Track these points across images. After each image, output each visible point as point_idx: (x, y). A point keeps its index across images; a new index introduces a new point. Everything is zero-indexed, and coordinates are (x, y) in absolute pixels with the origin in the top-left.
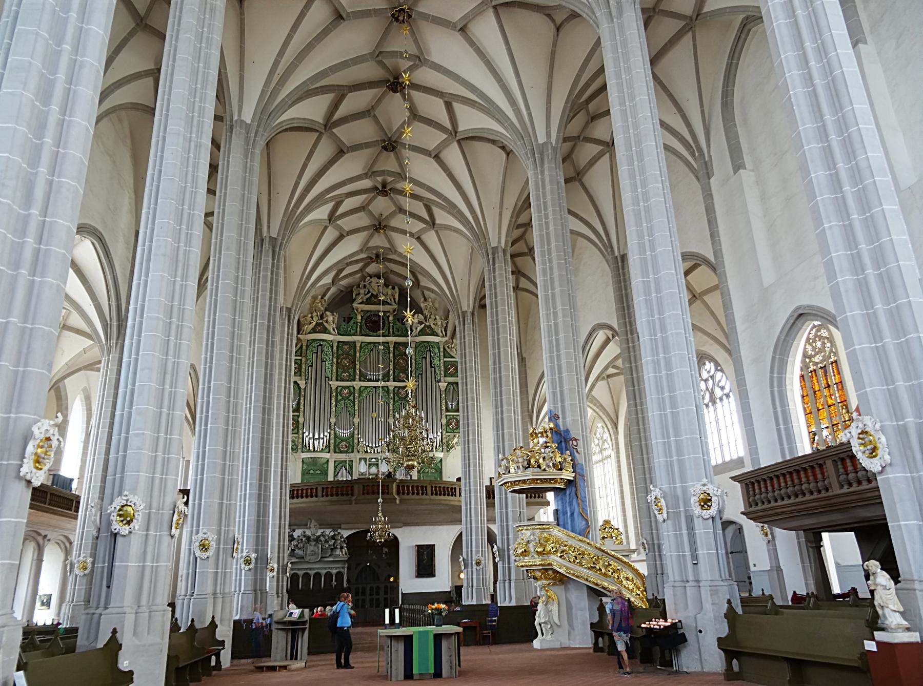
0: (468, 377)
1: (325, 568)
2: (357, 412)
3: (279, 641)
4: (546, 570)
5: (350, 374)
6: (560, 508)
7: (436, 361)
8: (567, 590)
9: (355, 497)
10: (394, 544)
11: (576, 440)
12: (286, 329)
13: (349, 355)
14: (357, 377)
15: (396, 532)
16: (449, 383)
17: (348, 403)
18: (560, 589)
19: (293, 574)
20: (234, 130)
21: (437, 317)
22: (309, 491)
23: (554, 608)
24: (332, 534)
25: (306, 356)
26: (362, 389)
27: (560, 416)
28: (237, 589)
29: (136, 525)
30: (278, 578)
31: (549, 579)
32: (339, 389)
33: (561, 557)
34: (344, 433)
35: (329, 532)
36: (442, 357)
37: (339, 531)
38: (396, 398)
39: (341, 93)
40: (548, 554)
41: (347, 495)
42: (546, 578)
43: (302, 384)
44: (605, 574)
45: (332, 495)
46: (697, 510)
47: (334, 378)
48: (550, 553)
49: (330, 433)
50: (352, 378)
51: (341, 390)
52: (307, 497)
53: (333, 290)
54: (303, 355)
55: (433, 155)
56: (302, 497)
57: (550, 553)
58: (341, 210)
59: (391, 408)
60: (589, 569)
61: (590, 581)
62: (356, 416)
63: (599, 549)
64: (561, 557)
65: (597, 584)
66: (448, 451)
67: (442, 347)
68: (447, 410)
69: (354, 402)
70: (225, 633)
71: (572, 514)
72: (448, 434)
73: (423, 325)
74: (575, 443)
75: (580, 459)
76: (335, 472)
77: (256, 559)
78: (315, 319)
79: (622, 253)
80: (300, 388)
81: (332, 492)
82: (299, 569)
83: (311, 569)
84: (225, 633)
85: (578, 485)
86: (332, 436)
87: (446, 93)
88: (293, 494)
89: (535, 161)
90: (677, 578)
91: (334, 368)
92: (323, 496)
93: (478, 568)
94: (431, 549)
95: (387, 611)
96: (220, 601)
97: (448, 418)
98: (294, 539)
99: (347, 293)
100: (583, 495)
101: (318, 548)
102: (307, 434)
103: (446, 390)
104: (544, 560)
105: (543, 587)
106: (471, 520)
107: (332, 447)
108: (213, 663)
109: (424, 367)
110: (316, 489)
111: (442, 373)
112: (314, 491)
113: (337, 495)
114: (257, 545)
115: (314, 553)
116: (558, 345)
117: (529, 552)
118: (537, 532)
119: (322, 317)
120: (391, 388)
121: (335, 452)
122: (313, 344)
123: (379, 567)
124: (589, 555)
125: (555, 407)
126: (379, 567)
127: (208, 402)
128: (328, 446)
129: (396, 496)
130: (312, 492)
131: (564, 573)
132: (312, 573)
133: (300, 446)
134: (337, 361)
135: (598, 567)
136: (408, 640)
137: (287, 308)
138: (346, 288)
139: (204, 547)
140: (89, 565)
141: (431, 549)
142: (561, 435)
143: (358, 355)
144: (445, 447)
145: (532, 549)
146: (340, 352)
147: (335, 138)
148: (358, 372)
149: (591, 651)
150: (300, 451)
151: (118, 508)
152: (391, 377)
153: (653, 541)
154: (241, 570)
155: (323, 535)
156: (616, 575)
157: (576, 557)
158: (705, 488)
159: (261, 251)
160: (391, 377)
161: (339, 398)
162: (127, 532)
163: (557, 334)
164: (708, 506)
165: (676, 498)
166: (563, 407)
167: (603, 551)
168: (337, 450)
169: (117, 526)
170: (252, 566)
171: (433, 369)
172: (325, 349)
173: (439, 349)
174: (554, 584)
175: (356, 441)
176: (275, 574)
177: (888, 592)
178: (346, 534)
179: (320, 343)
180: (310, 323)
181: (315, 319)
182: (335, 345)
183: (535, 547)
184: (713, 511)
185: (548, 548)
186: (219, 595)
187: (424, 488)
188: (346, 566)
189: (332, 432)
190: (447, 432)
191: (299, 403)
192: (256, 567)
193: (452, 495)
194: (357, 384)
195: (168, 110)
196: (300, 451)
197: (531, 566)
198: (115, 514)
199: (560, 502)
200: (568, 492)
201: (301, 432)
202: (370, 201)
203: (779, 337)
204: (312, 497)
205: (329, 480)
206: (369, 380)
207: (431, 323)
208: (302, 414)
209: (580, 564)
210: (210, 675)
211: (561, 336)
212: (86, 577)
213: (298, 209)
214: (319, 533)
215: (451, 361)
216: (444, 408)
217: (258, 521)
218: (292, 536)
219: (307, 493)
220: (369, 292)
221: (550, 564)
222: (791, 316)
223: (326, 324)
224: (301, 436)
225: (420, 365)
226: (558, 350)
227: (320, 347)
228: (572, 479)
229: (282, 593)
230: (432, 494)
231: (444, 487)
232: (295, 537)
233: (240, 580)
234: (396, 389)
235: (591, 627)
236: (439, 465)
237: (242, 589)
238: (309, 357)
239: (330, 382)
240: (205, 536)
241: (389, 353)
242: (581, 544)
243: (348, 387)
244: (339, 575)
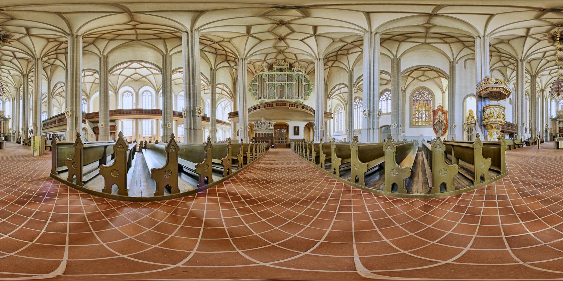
24: (269, 122)
115: (264, 127)
120: (287, 84)
132: (264, 133)
216: (304, 89)
244: (272, 134)
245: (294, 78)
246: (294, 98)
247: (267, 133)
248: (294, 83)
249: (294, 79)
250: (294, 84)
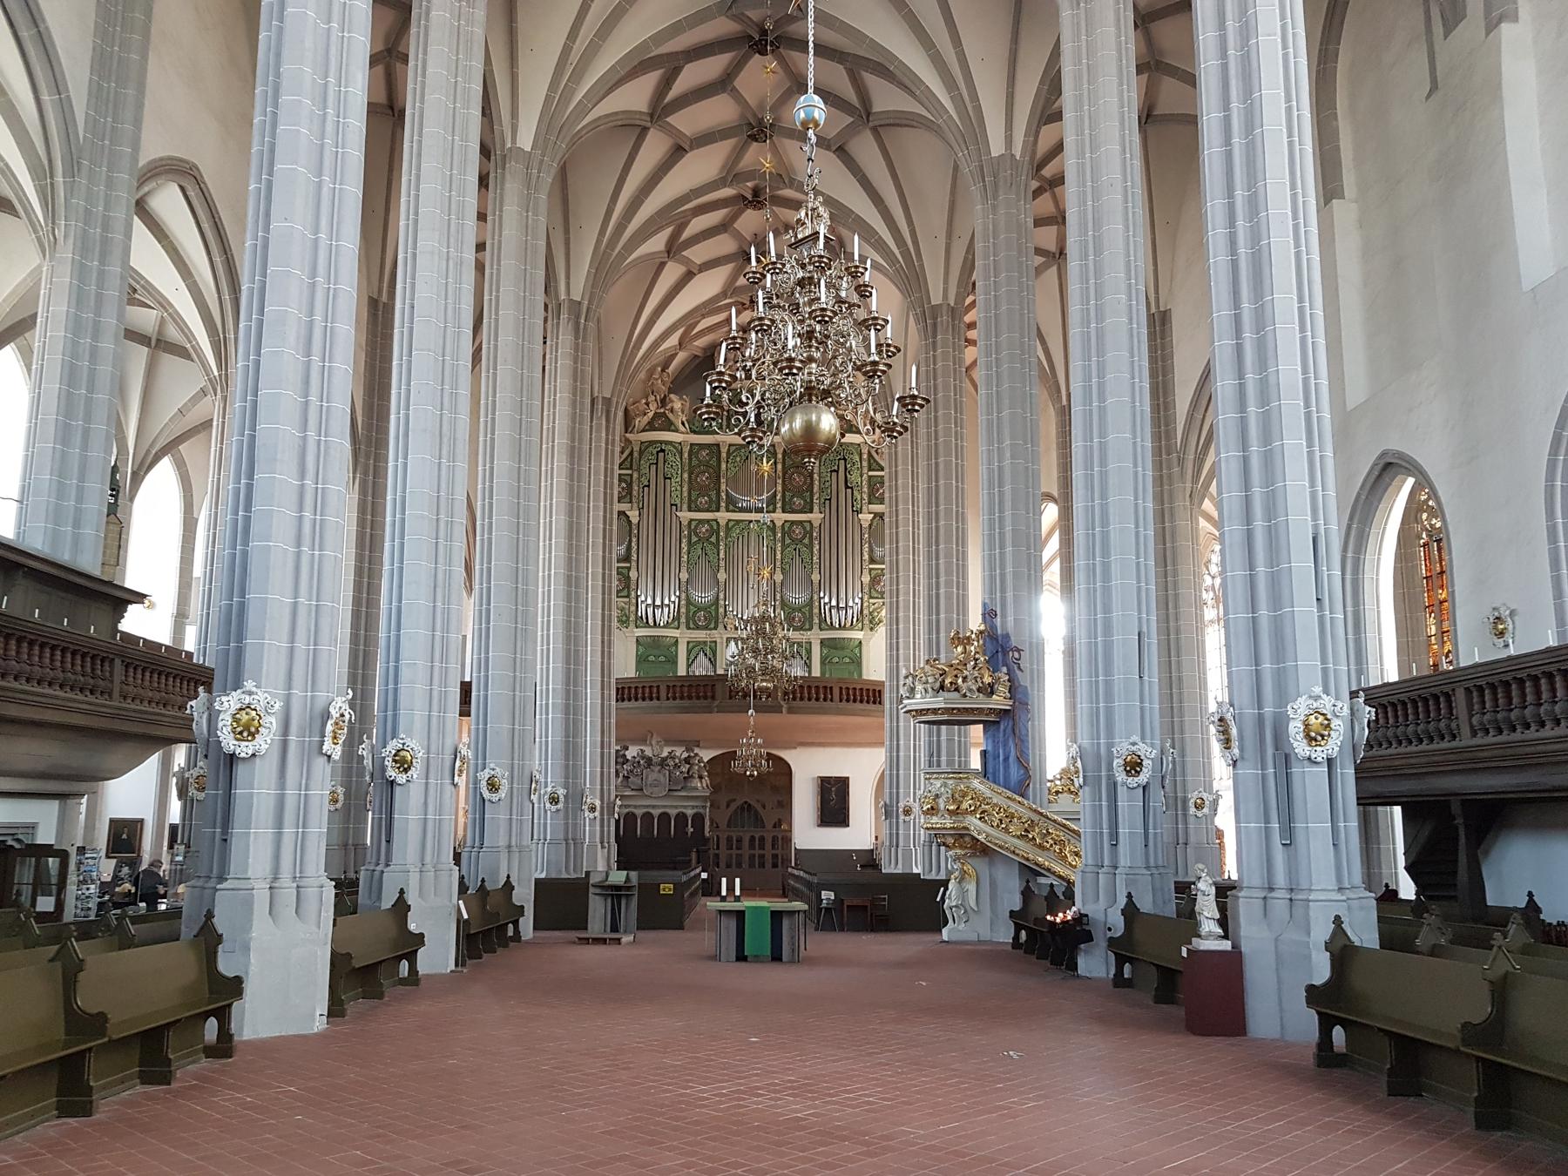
0: (900, 512)
1: (676, 807)
2: (722, 563)
3: (597, 909)
4: (962, 836)
5: (711, 500)
6: (990, 748)
7: (854, 478)
8: (991, 864)
9: (716, 703)
10: (784, 772)
11: (1019, 651)
12: (604, 435)
13: (708, 466)
14: (723, 504)
15: (786, 755)
16: (876, 515)
17: (708, 547)
18: (981, 864)
19: (628, 813)
20: (507, 165)
22: (647, 690)
23: (972, 887)
24: (685, 755)
25: (639, 470)
26: (730, 525)
27: (998, 613)
28: (542, 837)
29: (414, 773)
30: (602, 820)
31: (966, 848)
32: (694, 524)
33: (980, 819)
34: (702, 596)
35: (680, 752)
36: (865, 470)
37: (697, 750)
38: (788, 541)
39: (672, 65)
40: (962, 814)
41: (705, 698)
42: (961, 847)
43: (634, 515)
44: (1041, 847)
45: (682, 698)
46: (1120, 776)
47: (685, 507)
48: (966, 812)
49: (679, 597)
50: (714, 506)
51: (696, 527)
52: (644, 699)
53: (682, 356)
54: (635, 467)
55: (834, 148)
56: (636, 700)
57: (966, 812)
58: (686, 234)
59: (779, 556)
60: (1018, 837)
61: (1018, 855)
62: (722, 570)
63: (1035, 811)
64: (980, 819)
65: (1027, 859)
66: (871, 629)
67: (865, 451)
68: (872, 561)
69: (717, 546)
70: (524, 895)
71: (1006, 759)
72: (871, 601)
74: (1016, 655)
75: (1023, 679)
76: (688, 659)
77: (566, 797)
78: (653, 407)
79: (1162, 309)
80: (630, 522)
81: (682, 692)
82: (635, 807)
83: (654, 807)
84: (524, 895)
85: (1017, 717)
86: (683, 602)
87: (849, 54)
88: (623, 694)
89: (985, 186)
90: (1090, 862)
91: (685, 489)
92: (668, 699)
93: (907, 818)
94: (843, 783)
95: (724, 880)
96: (516, 856)
97: (874, 573)
98: (628, 760)
99: (706, 358)
100: (1024, 732)
101: (665, 775)
102: (643, 598)
103: (870, 525)
104: (959, 821)
105: (956, 859)
106: (898, 745)
107: (683, 620)
108: (510, 933)
109: (834, 487)
110: (658, 687)
111: (865, 496)
112: (655, 690)
113: (690, 698)
114: (567, 777)
115: (656, 784)
116: (1001, 502)
117: (938, 810)
118: (950, 782)
119: (663, 402)
120: (779, 524)
121: (688, 628)
122: (650, 449)
123: (764, 807)
124: (1020, 818)
125: (991, 599)
126: (764, 807)
127: (489, 589)
128: (677, 618)
129: (782, 703)
130: (651, 693)
131: (983, 840)
132: (656, 812)
133: (632, 618)
134: (690, 477)
135: (1031, 836)
136: (740, 915)
137: (603, 398)
138: (705, 349)
139: (493, 786)
140: (341, 798)
141: (843, 783)
142: (997, 640)
143: (724, 466)
144: (866, 621)
145: (942, 806)
146: (695, 462)
147: (671, 131)
148: (723, 495)
149: (1010, 948)
150: (632, 625)
151: (393, 752)
152: (779, 505)
153: (1176, 792)
154: (546, 811)
155: (671, 756)
156: (1057, 848)
157: (1001, 820)
158: (1134, 748)
159: (558, 324)
160: (779, 505)
161: (694, 539)
162: (404, 781)
163: (1001, 485)
164: (1136, 771)
165: (1098, 755)
166: (1003, 599)
167: (1041, 814)
168: (692, 626)
169: (391, 773)
170: (560, 806)
171: (849, 491)
172: (670, 458)
173: (861, 455)
174: (973, 855)
175: (721, 610)
176: (597, 814)
177: (1206, 898)
178: (707, 755)
179: (662, 448)
180: (645, 414)
181: (653, 407)
182: (686, 450)
183: (947, 802)
184: (1143, 778)
185: (965, 806)
186: (514, 849)
187: (828, 690)
188: (708, 804)
189: (683, 596)
190: (871, 597)
191: (629, 548)
192: (566, 808)
193: (874, 703)
194: (723, 516)
195: (416, 213)
196: (632, 625)
197: (939, 829)
198: (390, 759)
199: (990, 741)
200: (1002, 727)
201: (633, 594)
202: (734, 218)
203: (1359, 495)
204: (651, 699)
205: (679, 674)
206: (742, 510)
208: (634, 564)
209: (1006, 830)
210: (506, 946)
211: (1007, 488)
212: (337, 814)
213: (613, 250)
214: (665, 754)
216: (866, 557)
217: (567, 743)
218: (624, 756)
219: (643, 693)
221: (965, 828)
222: (1375, 464)
223: (670, 416)
224: (634, 601)
225: (827, 484)
226: (1001, 511)
227: (661, 454)
228: (1008, 708)
229: (608, 843)
230: (841, 701)
231: (861, 689)
232: (629, 757)
233: (545, 824)
234: (787, 525)
235: (1011, 917)
236: (857, 651)
237: (548, 838)
238: (643, 471)
239: (678, 514)
240: (493, 773)
242: (1010, 803)
243: (708, 521)
244: (698, 818)
245: (816, 476)
246: (816, 620)
247: (673, 812)
248: (815, 517)
249: (816, 489)
250: (816, 524)
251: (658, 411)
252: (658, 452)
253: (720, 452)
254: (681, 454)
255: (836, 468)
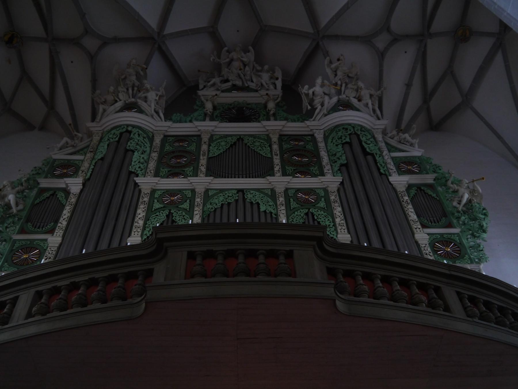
21: (361, 84)
26: (210, 193)
38: (293, 204)
73: (335, 99)
120: (280, 189)
122: (113, 132)
143: (204, 147)
171: (369, 157)
207: (350, 95)
215: (406, 157)
216: (413, 216)
220: (227, 81)
239: (138, 180)
241: (270, 146)
245: (323, 154)
251: (130, 100)
252: (121, 134)
253: (201, 139)
254: (151, 140)
255: (348, 140)
